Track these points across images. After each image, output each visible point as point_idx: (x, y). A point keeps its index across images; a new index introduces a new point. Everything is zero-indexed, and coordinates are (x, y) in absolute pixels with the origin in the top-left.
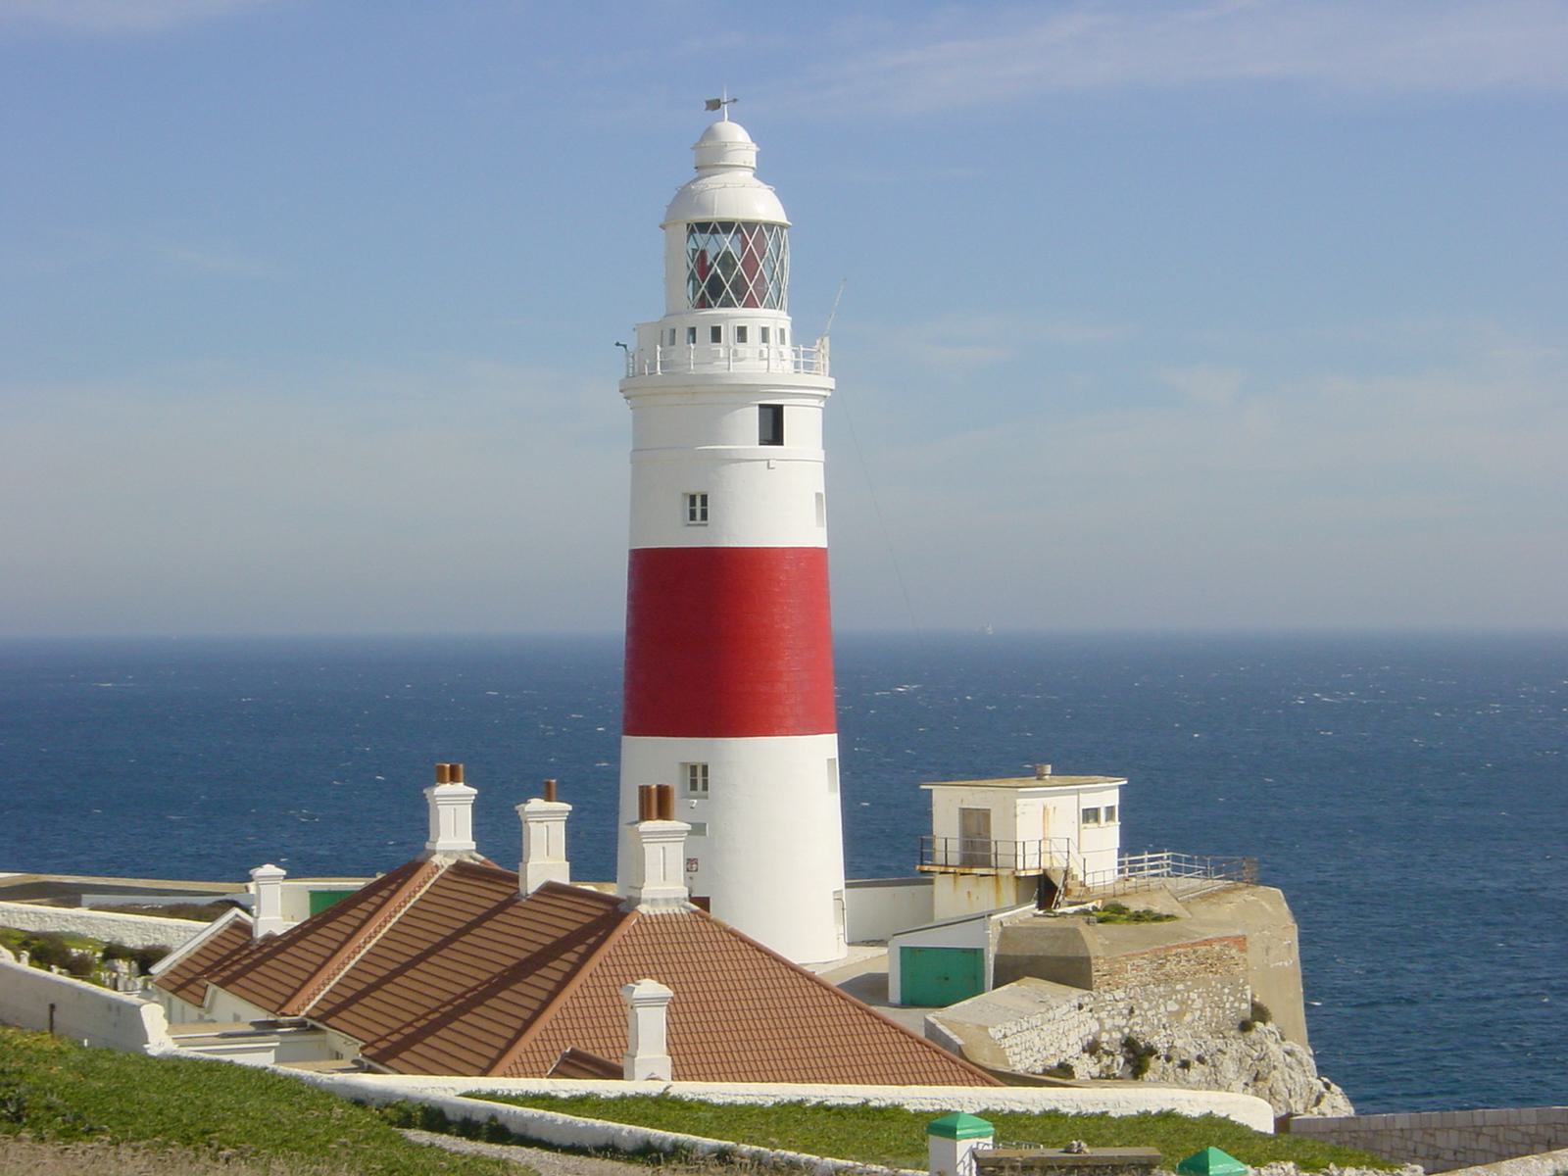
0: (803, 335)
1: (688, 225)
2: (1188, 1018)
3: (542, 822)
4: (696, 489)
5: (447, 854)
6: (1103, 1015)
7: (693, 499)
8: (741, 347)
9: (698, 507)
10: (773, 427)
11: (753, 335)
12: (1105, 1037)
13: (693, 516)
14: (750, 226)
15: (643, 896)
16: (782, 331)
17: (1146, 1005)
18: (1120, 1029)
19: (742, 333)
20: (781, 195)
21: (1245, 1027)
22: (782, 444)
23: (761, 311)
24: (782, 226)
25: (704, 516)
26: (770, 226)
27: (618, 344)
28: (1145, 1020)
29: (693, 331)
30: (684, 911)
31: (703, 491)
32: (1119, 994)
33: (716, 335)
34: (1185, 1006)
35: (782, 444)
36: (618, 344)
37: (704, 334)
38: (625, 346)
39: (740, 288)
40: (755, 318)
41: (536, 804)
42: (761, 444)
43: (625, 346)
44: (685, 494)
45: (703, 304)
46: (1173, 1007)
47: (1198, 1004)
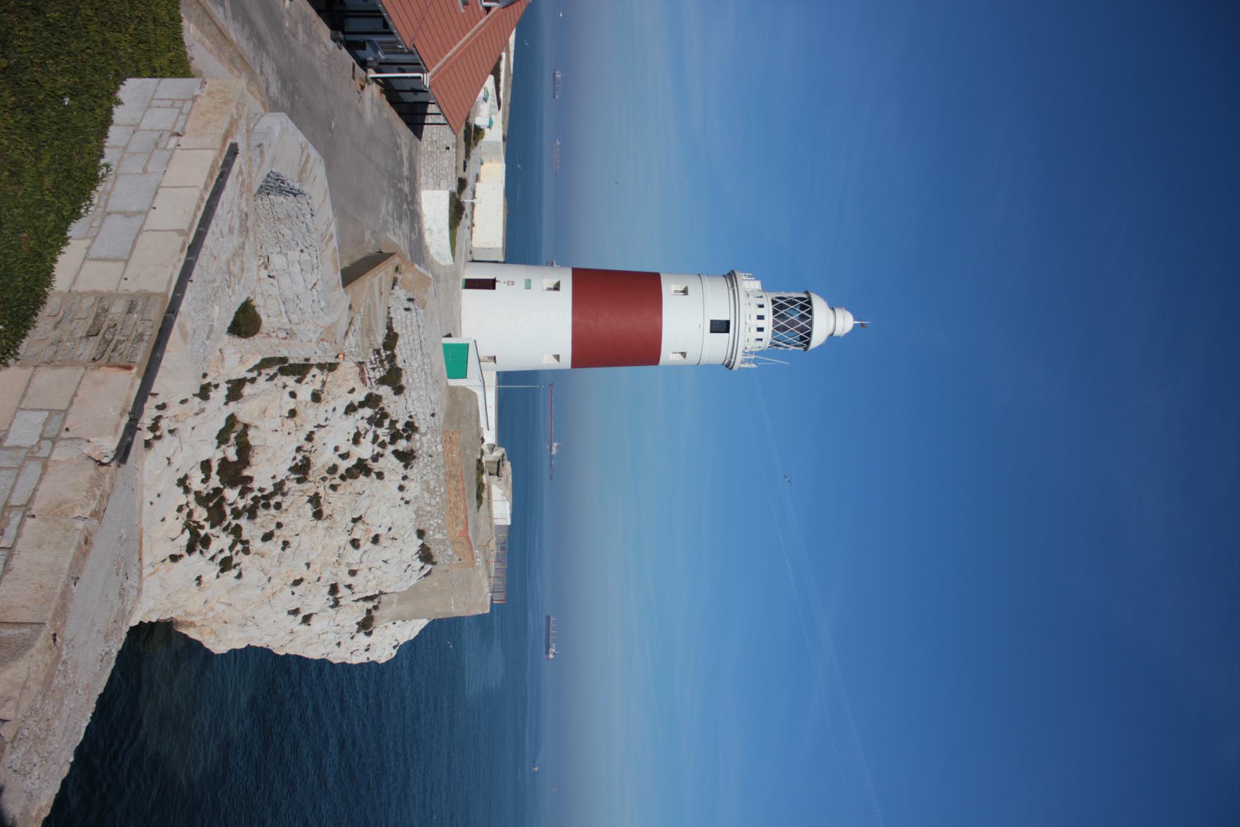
2: (426, 495)
6: (429, 436)
10: (721, 327)
12: (417, 436)
14: (811, 324)
17: (433, 466)
18: (422, 445)
20: (821, 346)
21: (421, 534)
22: (712, 331)
23: (771, 328)
24: (808, 343)
26: (809, 334)
28: (426, 465)
32: (440, 448)
33: (761, 306)
34: (432, 492)
35: (712, 331)
37: (761, 301)
39: (782, 317)
45: (774, 302)
46: (432, 484)
47: (433, 502)
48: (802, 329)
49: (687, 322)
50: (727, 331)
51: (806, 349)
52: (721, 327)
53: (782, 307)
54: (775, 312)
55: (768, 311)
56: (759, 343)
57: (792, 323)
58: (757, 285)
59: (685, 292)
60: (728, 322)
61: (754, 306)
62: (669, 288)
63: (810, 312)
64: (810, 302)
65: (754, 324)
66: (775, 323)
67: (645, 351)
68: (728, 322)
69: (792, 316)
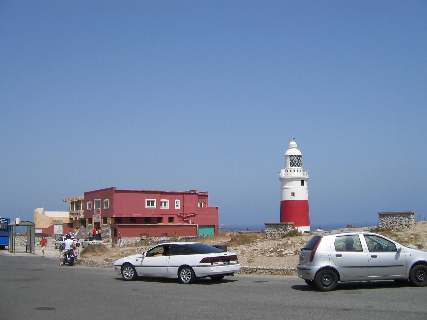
0: (304, 171)
4: (292, 192)
9: (293, 194)
14: (298, 156)
29: (291, 171)
33: (294, 171)
37: (293, 171)
40: (299, 168)
48: (299, 158)
49: (300, 193)
51: (301, 156)
52: (303, 184)
53: (294, 164)
54: (296, 166)
55: (294, 168)
56: (299, 171)
57: (298, 161)
58: (283, 171)
59: (293, 194)
61: (294, 173)
62: (288, 197)
63: (295, 156)
64: (292, 156)
65: (298, 173)
66: (299, 166)
67: (304, 204)
69: (295, 161)
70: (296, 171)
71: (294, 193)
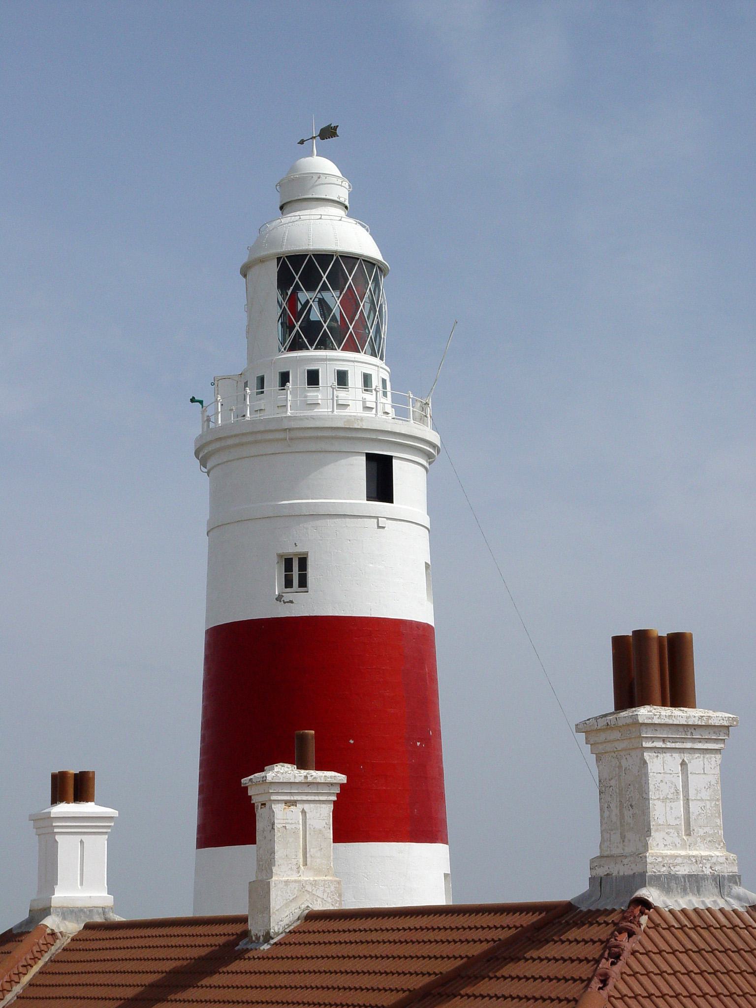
1: (279, 259)
3: (294, 803)
4: (290, 549)
5: (68, 912)
7: (288, 563)
8: (342, 394)
9: (296, 570)
11: (355, 380)
13: (288, 583)
15: (651, 870)
16: (384, 381)
19: (342, 378)
25: (303, 583)
27: (193, 400)
30: (736, 905)
31: (300, 549)
33: (313, 378)
36: (193, 400)
37: (298, 378)
38: (201, 402)
40: (357, 363)
41: (283, 772)
42: (369, 498)
43: (201, 402)
44: (280, 556)
45: (296, 346)
50: (390, 458)
60: (370, 457)
64: (296, 259)
68: (370, 457)
70: (327, 378)
71: (303, 562)
